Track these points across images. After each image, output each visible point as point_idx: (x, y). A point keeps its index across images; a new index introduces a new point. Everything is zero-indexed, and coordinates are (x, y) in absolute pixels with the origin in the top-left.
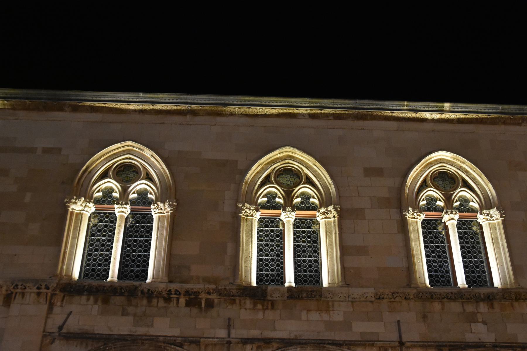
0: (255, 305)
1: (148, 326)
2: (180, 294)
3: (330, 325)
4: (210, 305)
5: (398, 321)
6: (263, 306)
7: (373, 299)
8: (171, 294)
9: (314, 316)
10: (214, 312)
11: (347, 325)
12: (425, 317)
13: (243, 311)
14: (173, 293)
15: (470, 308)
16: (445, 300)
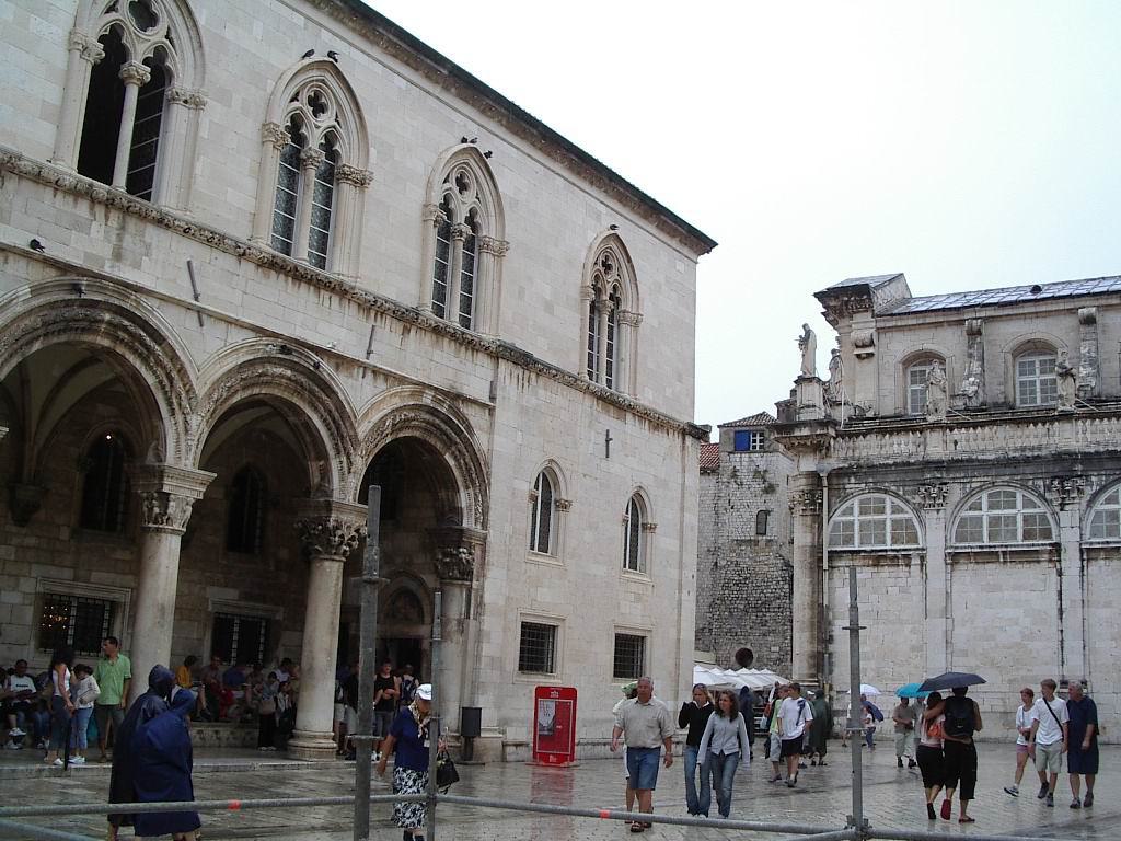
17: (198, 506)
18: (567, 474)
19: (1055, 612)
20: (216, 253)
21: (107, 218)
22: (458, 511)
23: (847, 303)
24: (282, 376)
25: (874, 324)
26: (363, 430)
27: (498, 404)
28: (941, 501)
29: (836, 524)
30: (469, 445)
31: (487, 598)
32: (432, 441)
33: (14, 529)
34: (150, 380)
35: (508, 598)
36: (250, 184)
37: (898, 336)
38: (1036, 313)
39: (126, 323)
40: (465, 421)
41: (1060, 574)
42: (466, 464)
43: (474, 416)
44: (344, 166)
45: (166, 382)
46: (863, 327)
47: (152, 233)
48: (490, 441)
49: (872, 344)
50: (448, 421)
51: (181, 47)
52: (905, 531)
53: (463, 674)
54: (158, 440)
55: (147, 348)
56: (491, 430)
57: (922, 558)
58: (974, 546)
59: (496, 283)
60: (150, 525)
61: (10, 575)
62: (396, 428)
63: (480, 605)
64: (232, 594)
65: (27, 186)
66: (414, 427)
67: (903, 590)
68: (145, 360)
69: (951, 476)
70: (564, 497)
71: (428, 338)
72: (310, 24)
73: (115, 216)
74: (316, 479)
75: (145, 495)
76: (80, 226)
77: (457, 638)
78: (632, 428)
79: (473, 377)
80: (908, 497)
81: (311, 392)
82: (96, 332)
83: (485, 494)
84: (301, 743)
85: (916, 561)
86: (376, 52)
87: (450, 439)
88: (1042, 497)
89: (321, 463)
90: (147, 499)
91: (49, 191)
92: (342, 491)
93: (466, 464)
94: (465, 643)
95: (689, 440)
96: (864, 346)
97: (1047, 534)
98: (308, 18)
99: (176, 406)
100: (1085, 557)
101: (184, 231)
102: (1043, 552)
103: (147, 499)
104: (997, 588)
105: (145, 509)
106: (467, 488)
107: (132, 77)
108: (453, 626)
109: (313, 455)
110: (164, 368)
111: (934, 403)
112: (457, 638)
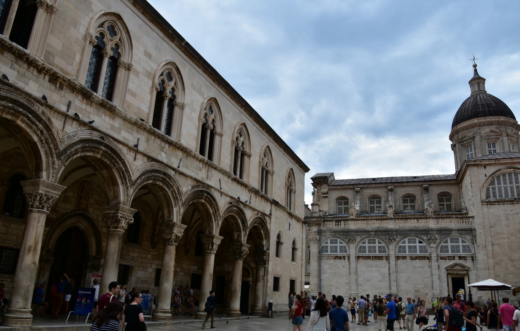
0: (83, 99)
1: (25, 84)
2: (48, 73)
3: (112, 127)
4: (61, 88)
5: (138, 139)
6: (87, 102)
7: (133, 123)
8: (44, 70)
9: (107, 119)
10: (63, 92)
11: (119, 131)
12: (148, 141)
13: (76, 99)
14: (46, 69)
15: (163, 144)
16: (157, 136)
17: (219, 246)
18: (283, 234)
19: (388, 274)
20: (224, 176)
21: (205, 167)
22: (263, 246)
23: (320, 181)
24: (235, 210)
25: (328, 188)
26: (249, 223)
27: (272, 217)
28: (354, 241)
29: (323, 247)
30: (267, 228)
31: (270, 270)
32: (259, 226)
33: (151, 250)
34: (211, 211)
35: (272, 270)
36: (229, 157)
37: (335, 191)
38: (376, 187)
39: (209, 196)
40: (266, 221)
41: (389, 263)
42: (266, 233)
43: (267, 218)
44: (246, 152)
45: (215, 212)
46: (325, 189)
47: (213, 171)
48: (270, 227)
49: (327, 193)
50: (263, 221)
51: (217, 119)
53: (263, 292)
54: (210, 228)
55: (212, 203)
56: (270, 223)
57: (349, 257)
59: (271, 183)
60: (208, 251)
61: (150, 263)
62: (254, 224)
63: (268, 272)
64: (196, 268)
65: (191, 158)
66: (257, 223)
67: (343, 266)
68: (211, 206)
69: (357, 234)
70: (281, 241)
71: (260, 198)
72: (240, 112)
73: (207, 166)
74: (236, 237)
75: (207, 243)
76: (200, 170)
78: (294, 222)
79: (265, 208)
80: (344, 240)
81: (240, 214)
82: (201, 198)
83: (269, 241)
84: (233, 312)
85: (347, 258)
86: (251, 119)
87: (263, 226)
88: (383, 241)
89: (238, 233)
90: (207, 244)
91: (195, 160)
92: (244, 240)
93: (266, 233)
94: (264, 283)
95: (304, 225)
96: (325, 194)
97: (385, 252)
98: (240, 111)
99: (216, 219)
100: (396, 258)
101: (219, 171)
102: (384, 257)
103: (207, 244)
104: (371, 266)
105: (207, 247)
106: (265, 239)
107: (209, 128)
108: (261, 278)
109: (236, 230)
110: (215, 208)
111: (352, 212)
112: (262, 281)
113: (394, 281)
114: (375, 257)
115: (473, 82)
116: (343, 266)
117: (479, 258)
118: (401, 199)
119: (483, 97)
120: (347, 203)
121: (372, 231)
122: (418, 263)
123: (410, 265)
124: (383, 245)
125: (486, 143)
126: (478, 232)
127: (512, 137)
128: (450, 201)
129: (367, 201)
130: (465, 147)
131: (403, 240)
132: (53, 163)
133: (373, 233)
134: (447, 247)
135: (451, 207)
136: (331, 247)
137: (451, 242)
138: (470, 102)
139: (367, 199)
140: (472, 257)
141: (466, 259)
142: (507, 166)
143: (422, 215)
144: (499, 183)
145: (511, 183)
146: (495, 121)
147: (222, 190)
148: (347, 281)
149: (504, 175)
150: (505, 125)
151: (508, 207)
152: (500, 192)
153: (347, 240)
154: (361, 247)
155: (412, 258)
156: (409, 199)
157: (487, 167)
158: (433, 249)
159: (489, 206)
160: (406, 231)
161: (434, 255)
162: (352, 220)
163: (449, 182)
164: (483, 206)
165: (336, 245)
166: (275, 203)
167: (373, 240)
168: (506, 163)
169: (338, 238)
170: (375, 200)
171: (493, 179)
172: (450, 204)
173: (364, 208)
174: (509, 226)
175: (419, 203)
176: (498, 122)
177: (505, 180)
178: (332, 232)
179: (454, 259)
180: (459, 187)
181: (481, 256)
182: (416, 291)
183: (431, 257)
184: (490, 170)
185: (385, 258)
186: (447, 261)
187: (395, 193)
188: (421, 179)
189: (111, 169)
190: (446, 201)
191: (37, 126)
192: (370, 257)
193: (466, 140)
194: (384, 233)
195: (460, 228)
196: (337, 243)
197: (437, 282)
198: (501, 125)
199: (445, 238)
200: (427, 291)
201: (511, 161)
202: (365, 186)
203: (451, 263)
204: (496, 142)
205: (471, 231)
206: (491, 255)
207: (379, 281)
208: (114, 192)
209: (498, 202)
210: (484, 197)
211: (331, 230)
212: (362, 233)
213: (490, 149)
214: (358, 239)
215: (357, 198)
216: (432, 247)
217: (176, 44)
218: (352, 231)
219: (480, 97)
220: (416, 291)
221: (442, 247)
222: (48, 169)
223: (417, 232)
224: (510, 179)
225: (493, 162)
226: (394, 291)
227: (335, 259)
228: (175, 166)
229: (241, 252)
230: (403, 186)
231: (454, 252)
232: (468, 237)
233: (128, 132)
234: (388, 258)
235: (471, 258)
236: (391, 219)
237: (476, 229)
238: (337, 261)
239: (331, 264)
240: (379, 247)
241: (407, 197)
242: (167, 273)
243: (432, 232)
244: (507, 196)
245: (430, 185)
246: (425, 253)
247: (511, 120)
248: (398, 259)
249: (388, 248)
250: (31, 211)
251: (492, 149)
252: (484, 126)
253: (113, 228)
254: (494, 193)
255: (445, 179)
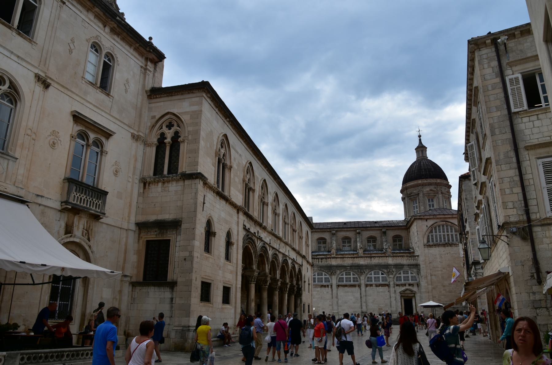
19: (360, 297)
41: (360, 289)
52: (327, 280)
57: (331, 286)
58: (343, 283)
67: (327, 293)
77: (299, 307)
79: (299, 260)
82: (284, 263)
104: (348, 292)
108: (299, 305)
112: (299, 307)
113: (364, 302)
114: (351, 285)
115: (419, 149)
116: (327, 293)
117: (422, 285)
118: (366, 240)
119: (425, 163)
120: (325, 243)
121: (348, 266)
122: (381, 289)
123: (375, 290)
124: (356, 276)
125: (427, 199)
126: (421, 266)
127: (445, 194)
128: (401, 242)
129: (340, 241)
130: (412, 200)
131: (370, 273)
132: (256, 261)
133: (349, 268)
134: (400, 277)
135: (401, 246)
136: (318, 278)
137: (403, 274)
138: (416, 166)
139: (341, 240)
140: (418, 284)
141: (413, 286)
142: (441, 220)
143: (382, 253)
144: (436, 232)
145: (444, 232)
146: (433, 183)
147: (290, 256)
148: (331, 303)
149: (439, 226)
150: (440, 186)
151: (442, 249)
152: (436, 238)
153: (330, 273)
154: (340, 278)
155: (377, 286)
156: (371, 240)
157: (428, 221)
158: (391, 279)
159: (429, 248)
160: (373, 266)
161: (392, 283)
162: (333, 258)
163: (401, 228)
164: (425, 248)
165: (321, 277)
166: (304, 257)
167: (349, 273)
168: (441, 218)
169: (323, 271)
170: (346, 241)
171: (432, 229)
172: (401, 244)
173: (338, 247)
174: (442, 263)
175: (379, 243)
176: (436, 183)
177: (439, 230)
178: (319, 267)
179: (405, 286)
180: (408, 231)
181: (423, 283)
182: (379, 309)
183: (390, 285)
184: (430, 222)
185: (358, 286)
186: (401, 287)
187: (361, 235)
188: (381, 225)
189: (264, 257)
190: (399, 242)
191: (253, 246)
192: (347, 285)
193: (413, 196)
194: (357, 267)
195: (409, 263)
196: (322, 275)
197: (394, 302)
198: (437, 186)
199: (399, 271)
200: (387, 309)
201: (444, 217)
202: (339, 230)
203: (403, 288)
204: (434, 198)
205: (417, 266)
206: (430, 283)
207: (354, 303)
208: (263, 268)
209: (435, 245)
210: (426, 241)
211: (317, 266)
212: (341, 268)
213: (429, 203)
214: (338, 272)
215: (333, 239)
216: (391, 278)
217: (276, 182)
218: (334, 266)
219: (423, 163)
220: (379, 309)
221: (397, 277)
222: (255, 264)
223: (380, 267)
224: (443, 229)
225: (432, 217)
226: (364, 309)
227: (321, 287)
228: (278, 249)
229: (294, 290)
230: (367, 230)
231: (405, 281)
232: (415, 270)
233: (268, 237)
234: (359, 286)
235: (416, 285)
236: (362, 257)
237: (420, 265)
238: (323, 288)
239: (318, 291)
240: (354, 278)
241: (370, 238)
242: (276, 306)
243: (391, 267)
244: (441, 241)
245: (387, 229)
246: (385, 281)
247: (445, 182)
248: (367, 286)
249: (360, 279)
250: (251, 283)
251: (431, 203)
252: (426, 185)
253: (265, 286)
254: (432, 239)
255: (398, 225)
